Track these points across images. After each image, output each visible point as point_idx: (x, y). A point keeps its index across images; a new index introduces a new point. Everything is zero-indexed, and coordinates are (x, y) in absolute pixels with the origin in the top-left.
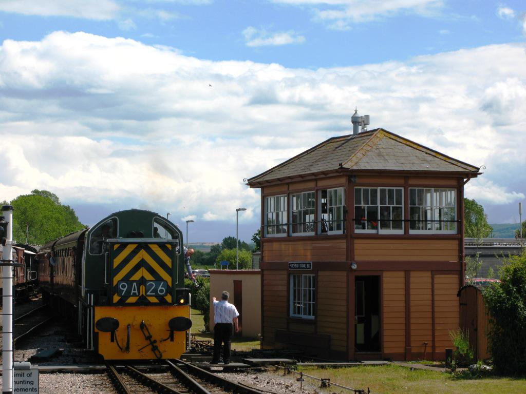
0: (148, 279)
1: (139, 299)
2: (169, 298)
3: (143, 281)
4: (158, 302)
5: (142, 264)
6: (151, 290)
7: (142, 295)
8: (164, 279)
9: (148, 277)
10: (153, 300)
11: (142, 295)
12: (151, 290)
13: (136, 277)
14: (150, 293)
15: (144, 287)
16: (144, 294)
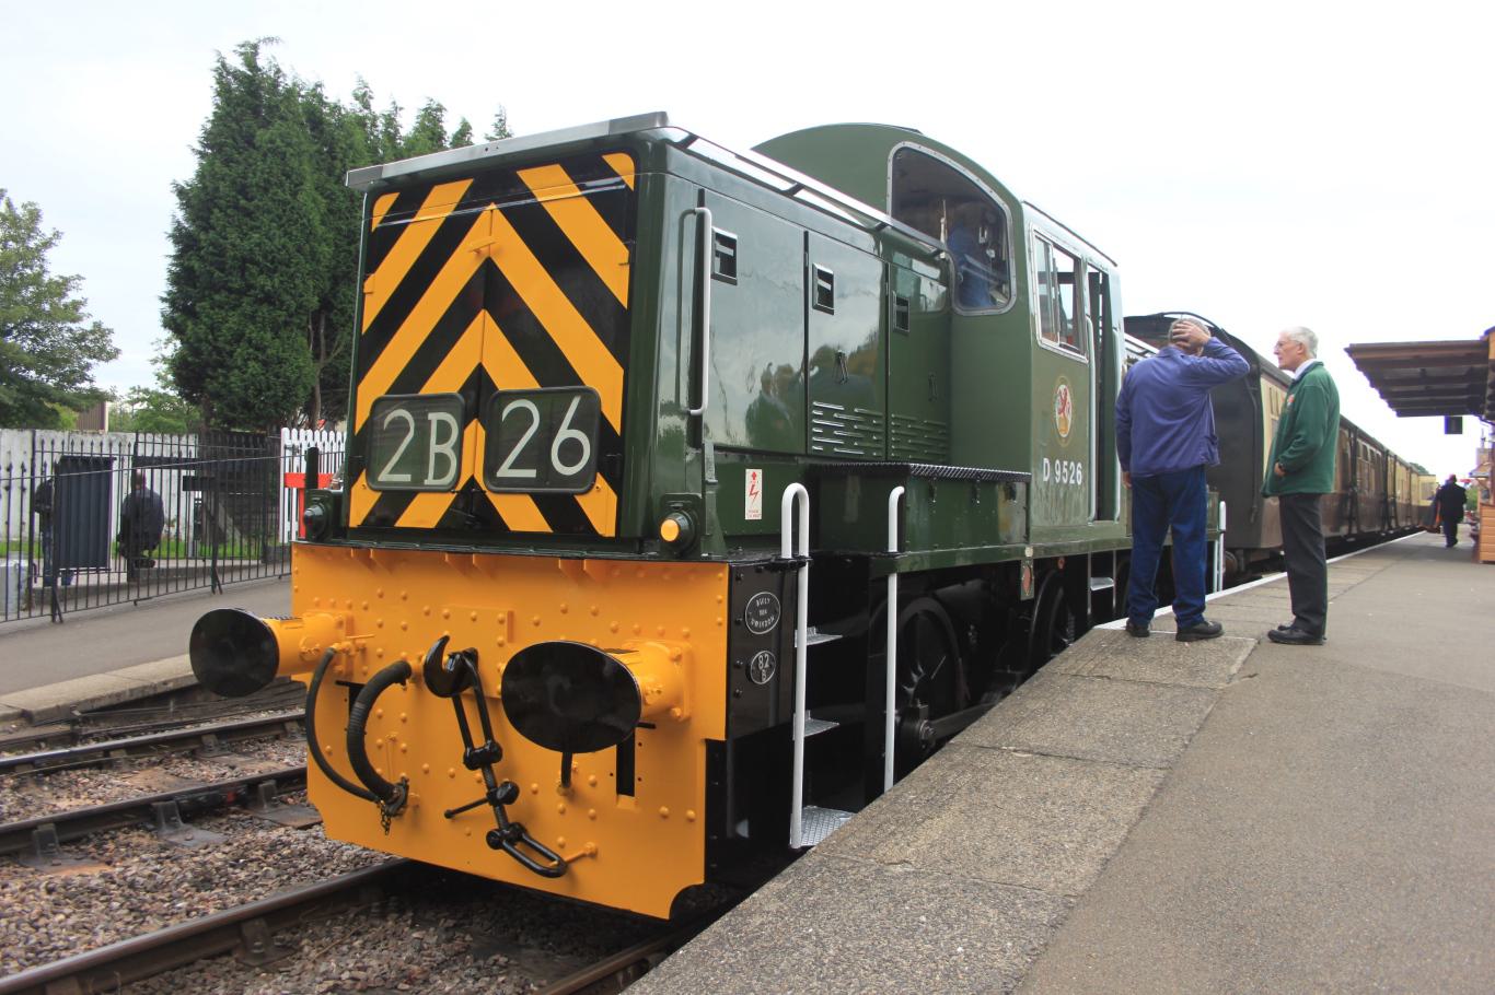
0: (502, 385)
1: (454, 505)
2: (600, 507)
3: (479, 395)
4: (546, 528)
5: (490, 290)
6: (395, 459)
7: (472, 480)
8: (588, 384)
9: (511, 373)
10: (521, 514)
11: (472, 480)
12: (395, 459)
13: (448, 378)
14: (391, 472)
15: (482, 433)
16: (480, 479)
